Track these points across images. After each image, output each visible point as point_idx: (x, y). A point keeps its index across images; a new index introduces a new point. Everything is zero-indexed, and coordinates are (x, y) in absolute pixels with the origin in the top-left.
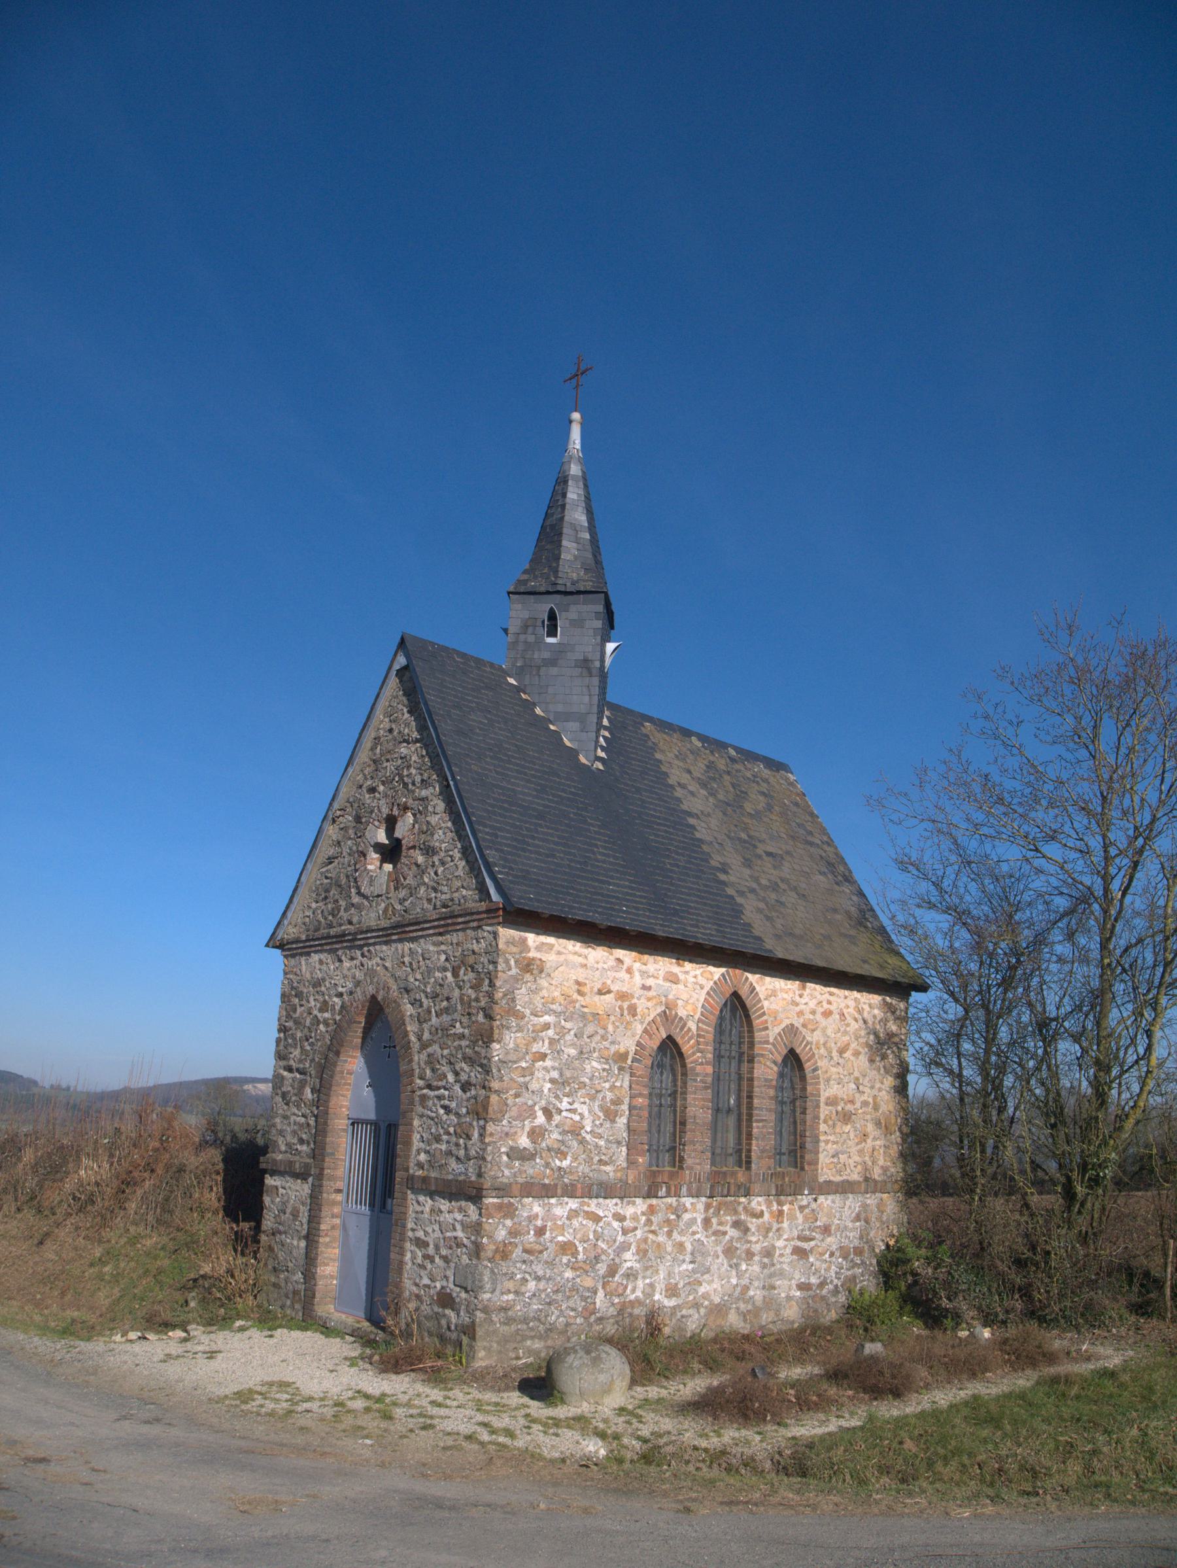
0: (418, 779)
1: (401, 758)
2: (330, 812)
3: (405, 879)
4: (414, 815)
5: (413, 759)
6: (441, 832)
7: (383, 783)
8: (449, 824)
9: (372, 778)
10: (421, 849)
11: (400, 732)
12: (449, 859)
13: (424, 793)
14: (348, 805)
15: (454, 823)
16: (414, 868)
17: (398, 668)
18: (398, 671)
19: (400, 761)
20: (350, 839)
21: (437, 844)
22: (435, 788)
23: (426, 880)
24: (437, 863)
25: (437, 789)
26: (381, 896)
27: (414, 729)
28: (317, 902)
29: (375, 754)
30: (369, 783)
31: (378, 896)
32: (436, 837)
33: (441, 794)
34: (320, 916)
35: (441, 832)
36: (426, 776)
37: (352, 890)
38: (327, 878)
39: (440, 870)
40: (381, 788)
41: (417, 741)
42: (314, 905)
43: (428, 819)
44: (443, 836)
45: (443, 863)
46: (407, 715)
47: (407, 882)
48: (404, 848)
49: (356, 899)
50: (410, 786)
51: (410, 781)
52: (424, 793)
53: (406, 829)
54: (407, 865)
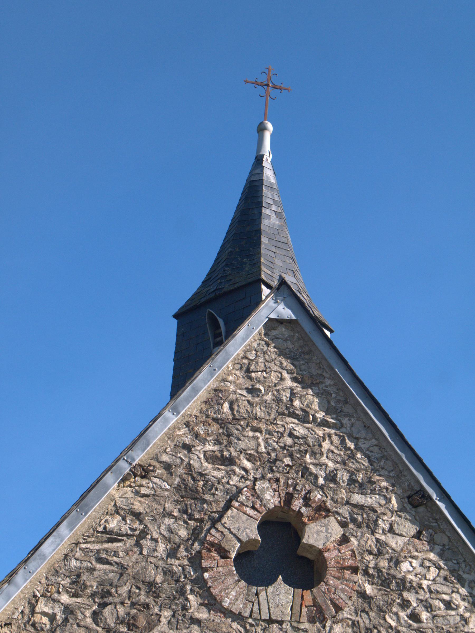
0: (343, 476)
1: (291, 435)
2: (122, 463)
3: (338, 609)
4: (343, 525)
5: (326, 445)
6: (415, 563)
7: (250, 458)
8: (432, 556)
9: (217, 442)
10: (366, 573)
11: (278, 400)
12: (442, 606)
13: (357, 498)
14: (157, 464)
15: (441, 555)
16: (355, 597)
17: (273, 316)
18: (270, 320)
19: (289, 441)
20: (170, 515)
21: (410, 577)
22: (389, 500)
23: (393, 624)
24: (414, 604)
25: (394, 501)
26: (281, 623)
27: (316, 406)
28: (75, 595)
29: (219, 412)
30: (210, 447)
31: (270, 621)
32: (405, 566)
33: (402, 509)
34: (89, 621)
35: (415, 563)
36: (360, 476)
37: (191, 597)
38: (100, 560)
39: (424, 616)
40: (248, 465)
41: (324, 423)
42: (65, 598)
43: (378, 536)
44: (419, 570)
45: (429, 607)
46: (289, 383)
47: (345, 614)
48: (331, 564)
49: (203, 615)
50: (321, 481)
51: (322, 473)
52: (357, 498)
53: (333, 539)
54: (343, 590)
